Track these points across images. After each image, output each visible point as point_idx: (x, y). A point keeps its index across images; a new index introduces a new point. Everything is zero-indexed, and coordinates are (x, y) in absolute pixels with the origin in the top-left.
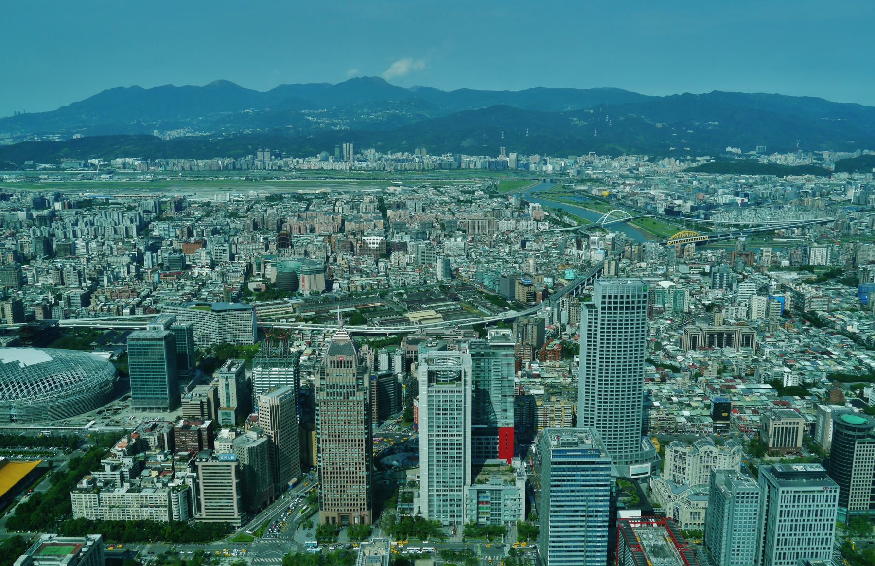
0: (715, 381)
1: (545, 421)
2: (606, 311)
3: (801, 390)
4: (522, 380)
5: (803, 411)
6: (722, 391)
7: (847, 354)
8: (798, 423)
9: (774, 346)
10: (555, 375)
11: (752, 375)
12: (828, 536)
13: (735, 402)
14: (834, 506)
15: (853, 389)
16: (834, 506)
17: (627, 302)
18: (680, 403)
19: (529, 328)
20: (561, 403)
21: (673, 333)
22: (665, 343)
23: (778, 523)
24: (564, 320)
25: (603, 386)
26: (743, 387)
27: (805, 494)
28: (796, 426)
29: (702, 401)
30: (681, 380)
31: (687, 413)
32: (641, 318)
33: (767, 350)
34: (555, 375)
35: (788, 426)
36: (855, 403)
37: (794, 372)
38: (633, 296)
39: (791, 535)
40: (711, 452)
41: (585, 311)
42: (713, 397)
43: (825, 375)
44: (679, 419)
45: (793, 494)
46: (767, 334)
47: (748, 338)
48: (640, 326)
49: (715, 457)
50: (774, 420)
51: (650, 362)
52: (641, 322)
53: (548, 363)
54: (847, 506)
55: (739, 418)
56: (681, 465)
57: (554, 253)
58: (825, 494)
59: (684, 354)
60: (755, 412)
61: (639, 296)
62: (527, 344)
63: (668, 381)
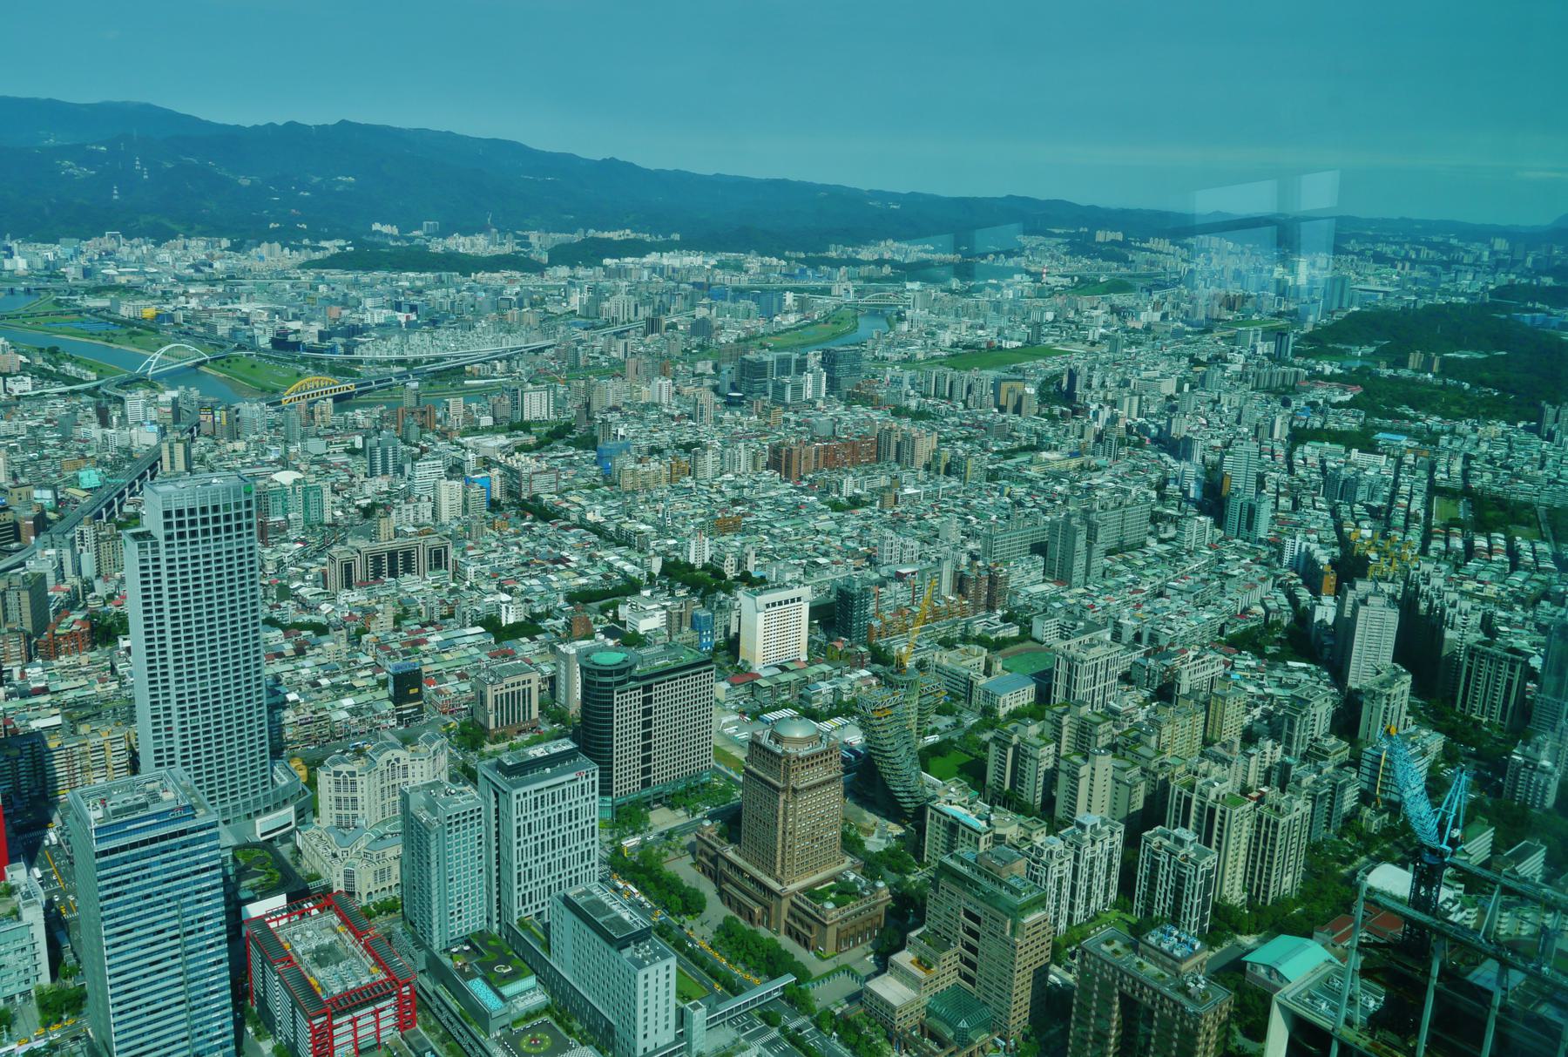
0: (391, 637)
1: (72, 777)
2: (176, 541)
4: (10, 704)
5: (535, 660)
6: (405, 653)
7: (591, 558)
9: (482, 562)
10: (82, 681)
11: (451, 615)
13: (429, 666)
15: (603, 610)
17: (216, 520)
18: (334, 686)
19: (11, 598)
20: (102, 735)
21: (308, 564)
22: (296, 585)
24: (88, 570)
25: (186, 684)
26: (439, 638)
29: (373, 676)
30: (333, 646)
32: (246, 546)
33: (471, 570)
34: (82, 681)
36: (609, 633)
37: (517, 600)
38: (226, 507)
41: (133, 546)
42: (391, 666)
43: (561, 596)
44: (335, 716)
46: (469, 543)
47: (438, 554)
48: (246, 560)
50: (492, 683)
51: (271, 623)
52: (246, 553)
53: (64, 660)
55: (438, 692)
57: (51, 438)
59: (332, 599)
60: (462, 677)
61: (238, 506)
62: (11, 631)
63: (309, 653)
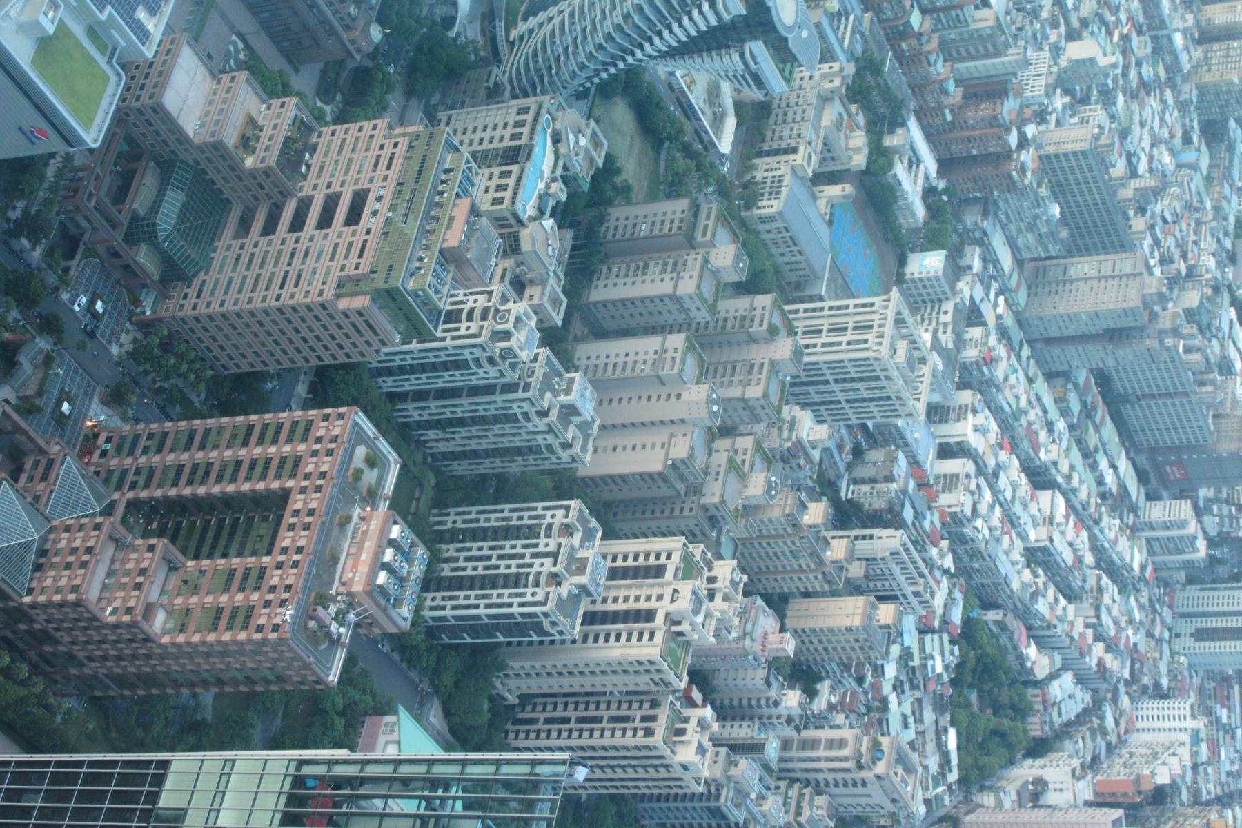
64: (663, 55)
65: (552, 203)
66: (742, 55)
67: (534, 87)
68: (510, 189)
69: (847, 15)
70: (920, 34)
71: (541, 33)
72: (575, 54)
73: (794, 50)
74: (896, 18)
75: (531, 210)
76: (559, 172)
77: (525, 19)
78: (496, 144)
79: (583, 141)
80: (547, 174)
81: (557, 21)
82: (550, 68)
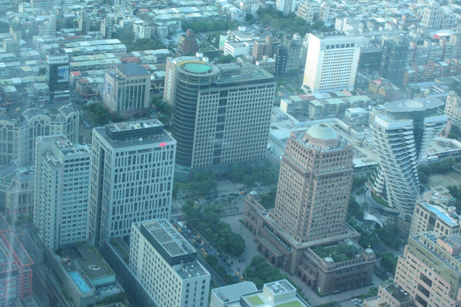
3: (153, 42)
8: (144, 81)
12: (166, 197)
14: (171, 163)
16: (171, 163)
23: (112, 190)
27: (140, 154)
28: (142, 84)
31: (17, 80)
35: (134, 85)
39: (127, 201)
40: (42, 122)
45: (128, 156)
49: (47, 128)
54: (189, 165)
56: (6, 142)
58: (162, 151)
64: (418, 155)
65: (455, 213)
66: (428, 127)
67: (412, 205)
68: (444, 226)
69: (432, 87)
70: (450, 64)
71: (393, 195)
72: (405, 185)
73: (433, 107)
74: (441, 71)
75: (454, 222)
76: (445, 207)
77: (387, 199)
78: (426, 225)
79: (437, 194)
80: (444, 211)
81: (391, 188)
82: (407, 196)
